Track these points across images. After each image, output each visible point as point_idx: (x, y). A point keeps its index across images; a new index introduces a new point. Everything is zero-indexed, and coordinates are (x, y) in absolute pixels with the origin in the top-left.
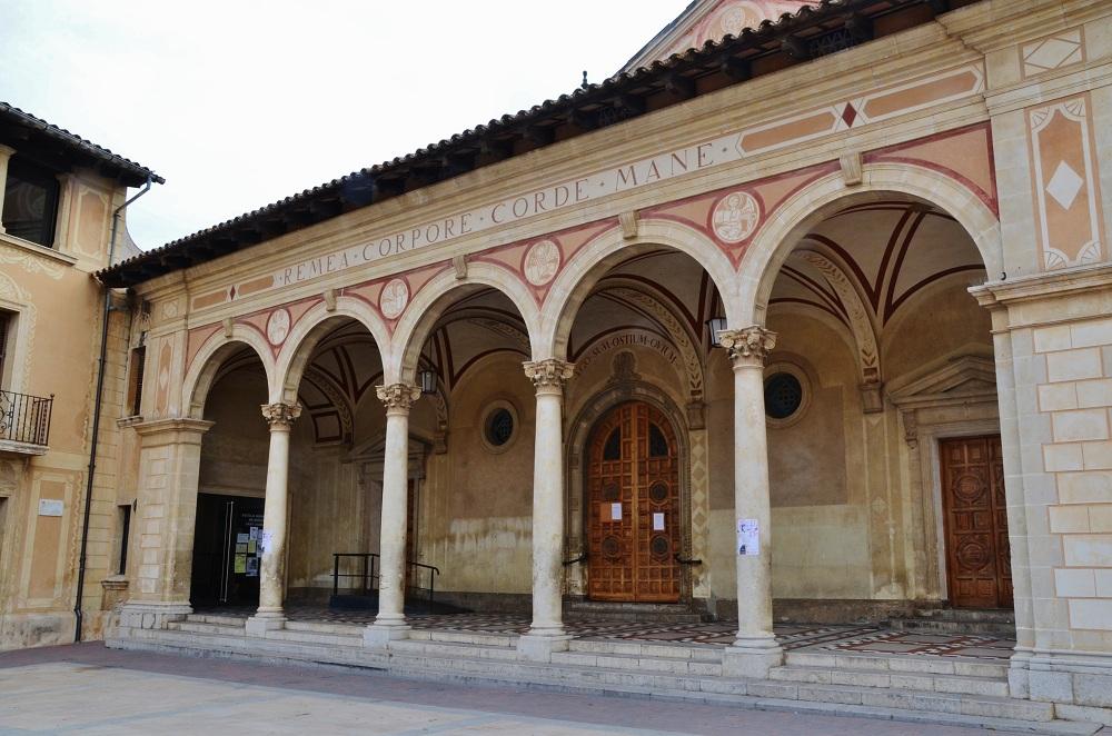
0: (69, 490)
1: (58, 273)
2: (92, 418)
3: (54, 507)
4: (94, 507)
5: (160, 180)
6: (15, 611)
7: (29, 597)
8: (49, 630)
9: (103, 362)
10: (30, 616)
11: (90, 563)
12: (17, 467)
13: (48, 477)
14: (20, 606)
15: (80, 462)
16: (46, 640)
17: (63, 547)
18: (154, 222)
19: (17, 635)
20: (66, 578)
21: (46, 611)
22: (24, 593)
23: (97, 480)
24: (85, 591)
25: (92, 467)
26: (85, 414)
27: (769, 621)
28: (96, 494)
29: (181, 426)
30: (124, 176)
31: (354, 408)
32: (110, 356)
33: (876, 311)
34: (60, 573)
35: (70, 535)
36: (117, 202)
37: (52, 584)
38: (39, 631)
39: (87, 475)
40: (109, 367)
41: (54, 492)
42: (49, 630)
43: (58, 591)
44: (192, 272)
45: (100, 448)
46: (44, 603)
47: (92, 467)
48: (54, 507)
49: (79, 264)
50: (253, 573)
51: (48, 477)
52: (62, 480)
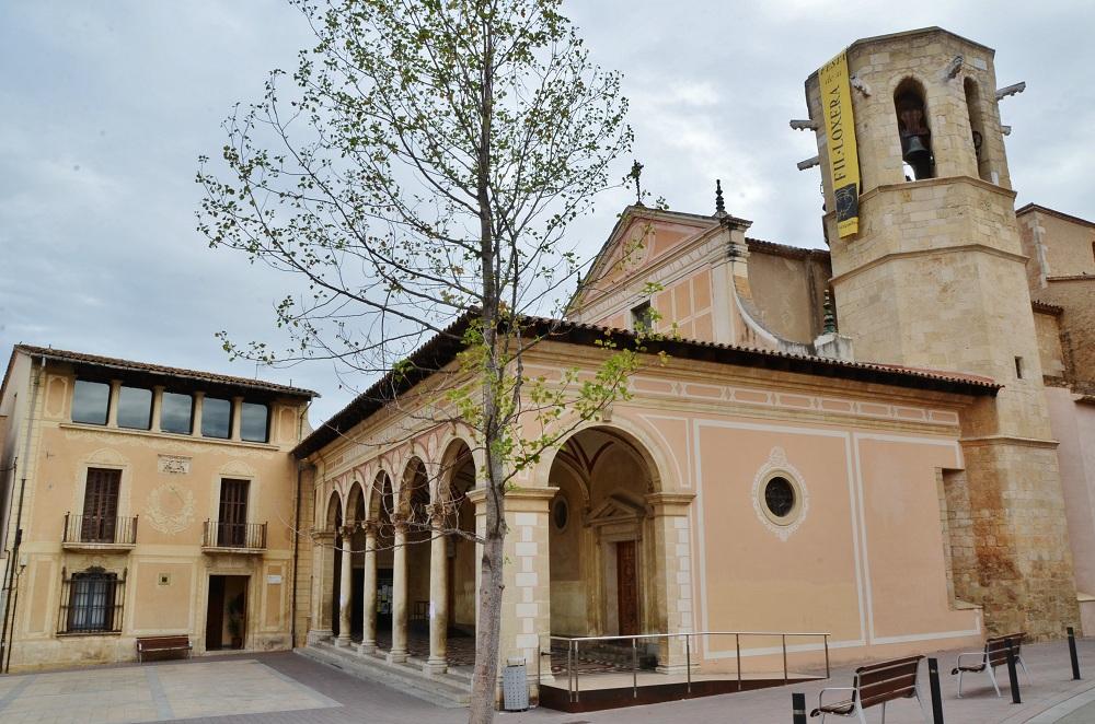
0: (284, 570)
1: (270, 456)
3: (276, 579)
4: (299, 578)
5: (317, 395)
6: (259, 633)
7: (266, 625)
8: (277, 643)
9: (299, 499)
11: (299, 607)
12: (255, 560)
13: (271, 564)
15: (289, 554)
16: (276, 648)
18: (318, 415)
19: (261, 645)
20: (286, 616)
21: (276, 633)
22: (263, 624)
23: (300, 563)
24: (297, 622)
25: (296, 556)
27: (443, 652)
28: (300, 571)
29: (323, 535)
30: (298, 399)
32: (303, 495)
33: (580, 464)
34: (282, 613)
35: (287, 593)
36: (302, 409)
37: (278, 619)
38: (272, 643)
40: (303, 501)
41: (276, 571)
42: (277, 643)
43: (282, 622)
44: (324, 451)
45: (300, 546)
46: (274, 628)
47: (296, 556)
48: (276, 579)
49: (282, 449)
50: (386, 611)
51: (271, 564)
52: (279, 564)
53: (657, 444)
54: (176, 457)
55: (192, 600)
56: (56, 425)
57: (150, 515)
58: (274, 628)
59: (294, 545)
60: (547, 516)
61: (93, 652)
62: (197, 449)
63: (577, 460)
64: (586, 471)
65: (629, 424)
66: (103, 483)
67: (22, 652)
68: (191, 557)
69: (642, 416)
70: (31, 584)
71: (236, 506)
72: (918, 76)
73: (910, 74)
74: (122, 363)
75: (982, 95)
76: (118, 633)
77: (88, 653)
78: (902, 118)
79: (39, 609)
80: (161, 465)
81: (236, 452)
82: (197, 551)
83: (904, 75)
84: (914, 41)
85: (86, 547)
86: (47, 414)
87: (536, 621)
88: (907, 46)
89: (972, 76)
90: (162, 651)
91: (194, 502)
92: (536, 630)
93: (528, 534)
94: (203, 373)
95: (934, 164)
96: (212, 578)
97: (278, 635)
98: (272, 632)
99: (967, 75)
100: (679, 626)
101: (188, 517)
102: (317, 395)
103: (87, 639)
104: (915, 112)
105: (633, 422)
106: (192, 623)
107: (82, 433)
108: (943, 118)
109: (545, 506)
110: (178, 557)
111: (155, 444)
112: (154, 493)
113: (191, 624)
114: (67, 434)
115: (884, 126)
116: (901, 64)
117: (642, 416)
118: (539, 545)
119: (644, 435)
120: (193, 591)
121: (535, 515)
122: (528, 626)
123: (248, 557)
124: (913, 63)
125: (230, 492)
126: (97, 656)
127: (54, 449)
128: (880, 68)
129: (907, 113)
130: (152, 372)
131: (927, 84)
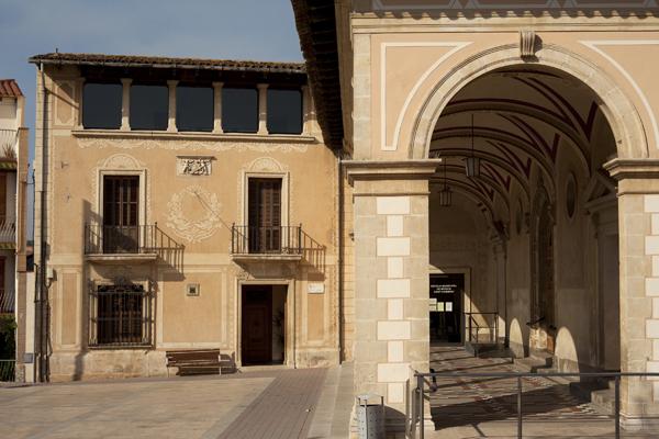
2: (337, 232)
3: (317, 287)
4: (346, 286)
6: (301, 347)
7: (309, 339)
8: (322, 358)
10: (311, 350)
14: (304, 344)
17: (326, 311)
19: (303, 360)
20: (331, 329)
21: (320, 347)
26: (330, 232)
31: (493, 204)
33: (573, 126)
34: (326, 326)
37: (322, 332)
38: (316, 359)
39: (337, 267)
42: (322, 358)
43: (326, 336)
46: (319, 343)
53: (536, 72)
54: (196, 158)
55: (224, 316)
56: (69, 133)
57: (172, 222)
58: (319, 343)
59: (338, 249)
60: (425, 202)
61: (124, 366)
62: (219, 146)
63: (567, 120)
64: (583, 136)
65: (567, 58)
66: (120, 191)
67: (58, 363)
68: (73, 266)
69: (589, 44)
70: (60, 296)
71: (125, 206)
74: (134, 60)
76: (154, 348)
77: (121, 367)
79: (68, 324)
80: (181, 166)
81: (263, 147)
82: (228, 259)
85: (105, 258)
86: (58, 122)
87: (408, 346)
90: (194, 364)
91: (220, 205)
92: (408, 358)
93: (396, 226)
94: (177, 60)
96: (244, 287)
97: (323, 350)
98: (315, 347)
100: (648, 359)
101: (214, 223)
102: (36, 60)
103: (117, 352)
105: (572, 54)
106: (228, 340)
107: (95, 140)
109: (423, 186)
110: (205, 266)
111: (172, 145)
112: (175, 198)
113: (224, 338)
114: (81, 143)
117: (589, 44)
118: (413, 240)
119: (591, 72)
120: (224, 302)
121: (408, 198)
122: (396, 352)
123: (284, 264)
125: (125, 190)
126: (129, 369)
127: (69, 162)
130: (155, 66)
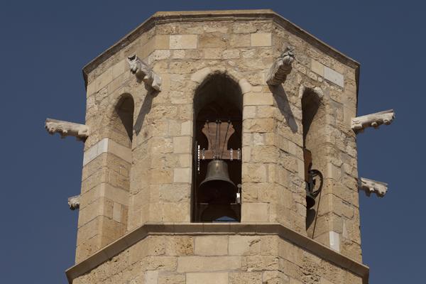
72: (234, 73)
73: (222, 69)
75: (329, 119)
78: (204, 131)
83: (215, 69)
84: (236, 25)
88: (224, 30)
89: (317, 89)
95: (239, 206)
99: (309, 86)
104: (224, 125)
108: (260, 138)
115: (171, 137)
116: (212, 53)
124: (230, 54)
128: (176, 55)
129: (213, 126)
131: (245, 86)
